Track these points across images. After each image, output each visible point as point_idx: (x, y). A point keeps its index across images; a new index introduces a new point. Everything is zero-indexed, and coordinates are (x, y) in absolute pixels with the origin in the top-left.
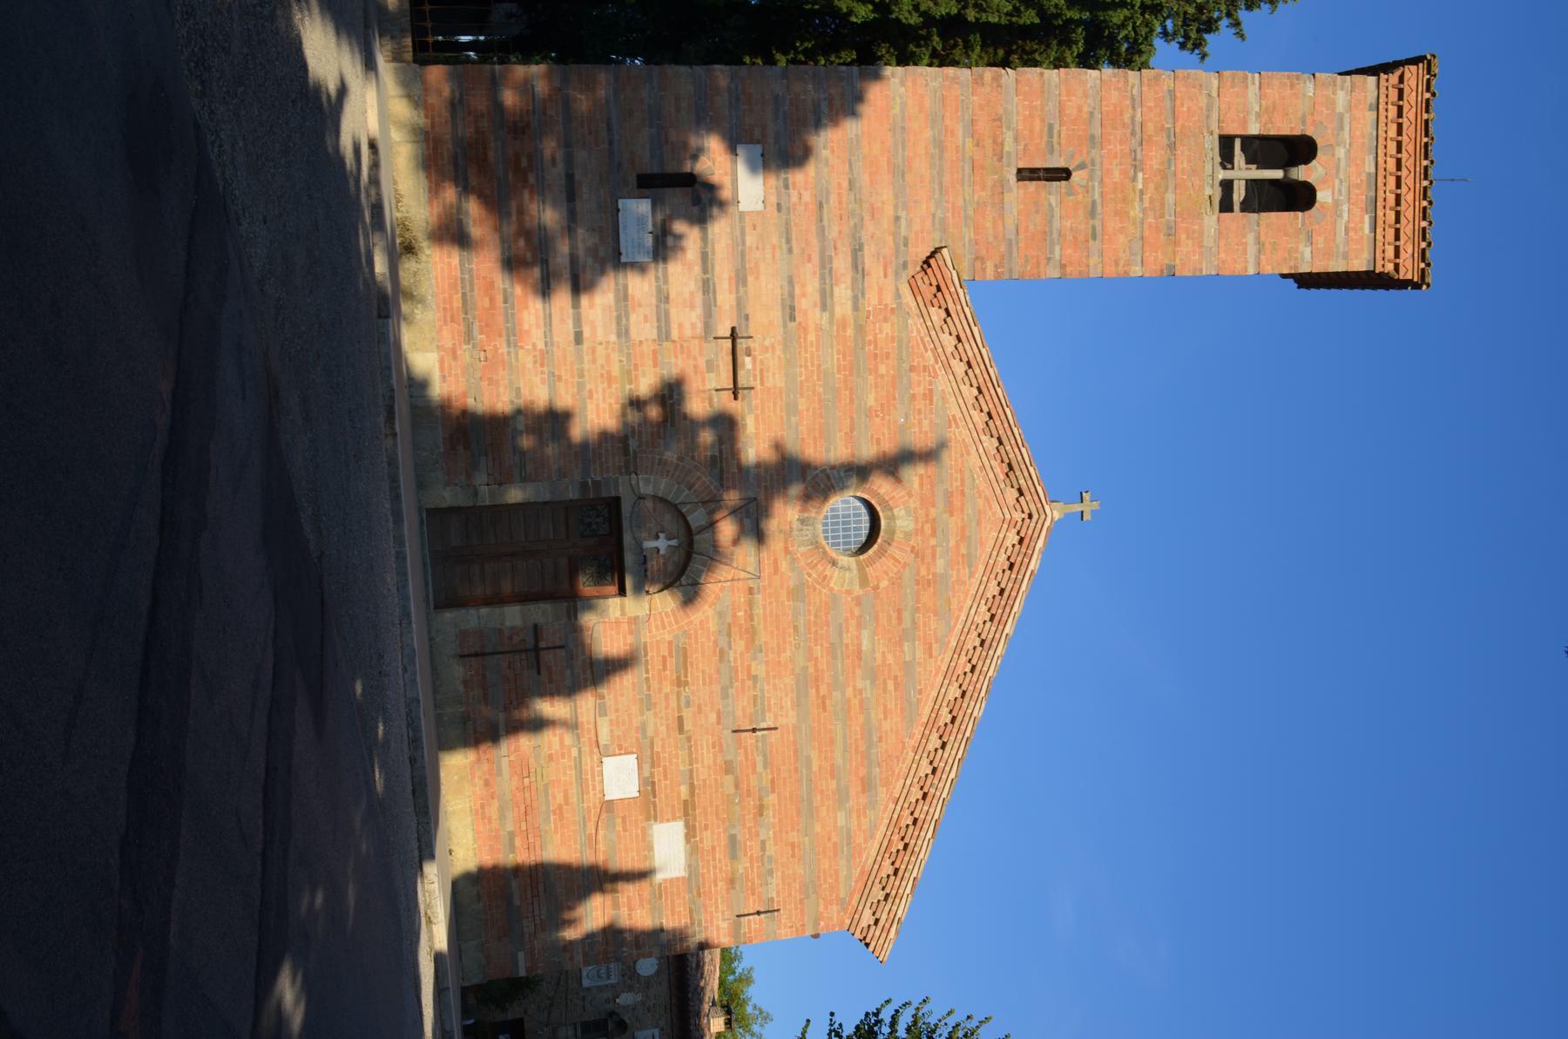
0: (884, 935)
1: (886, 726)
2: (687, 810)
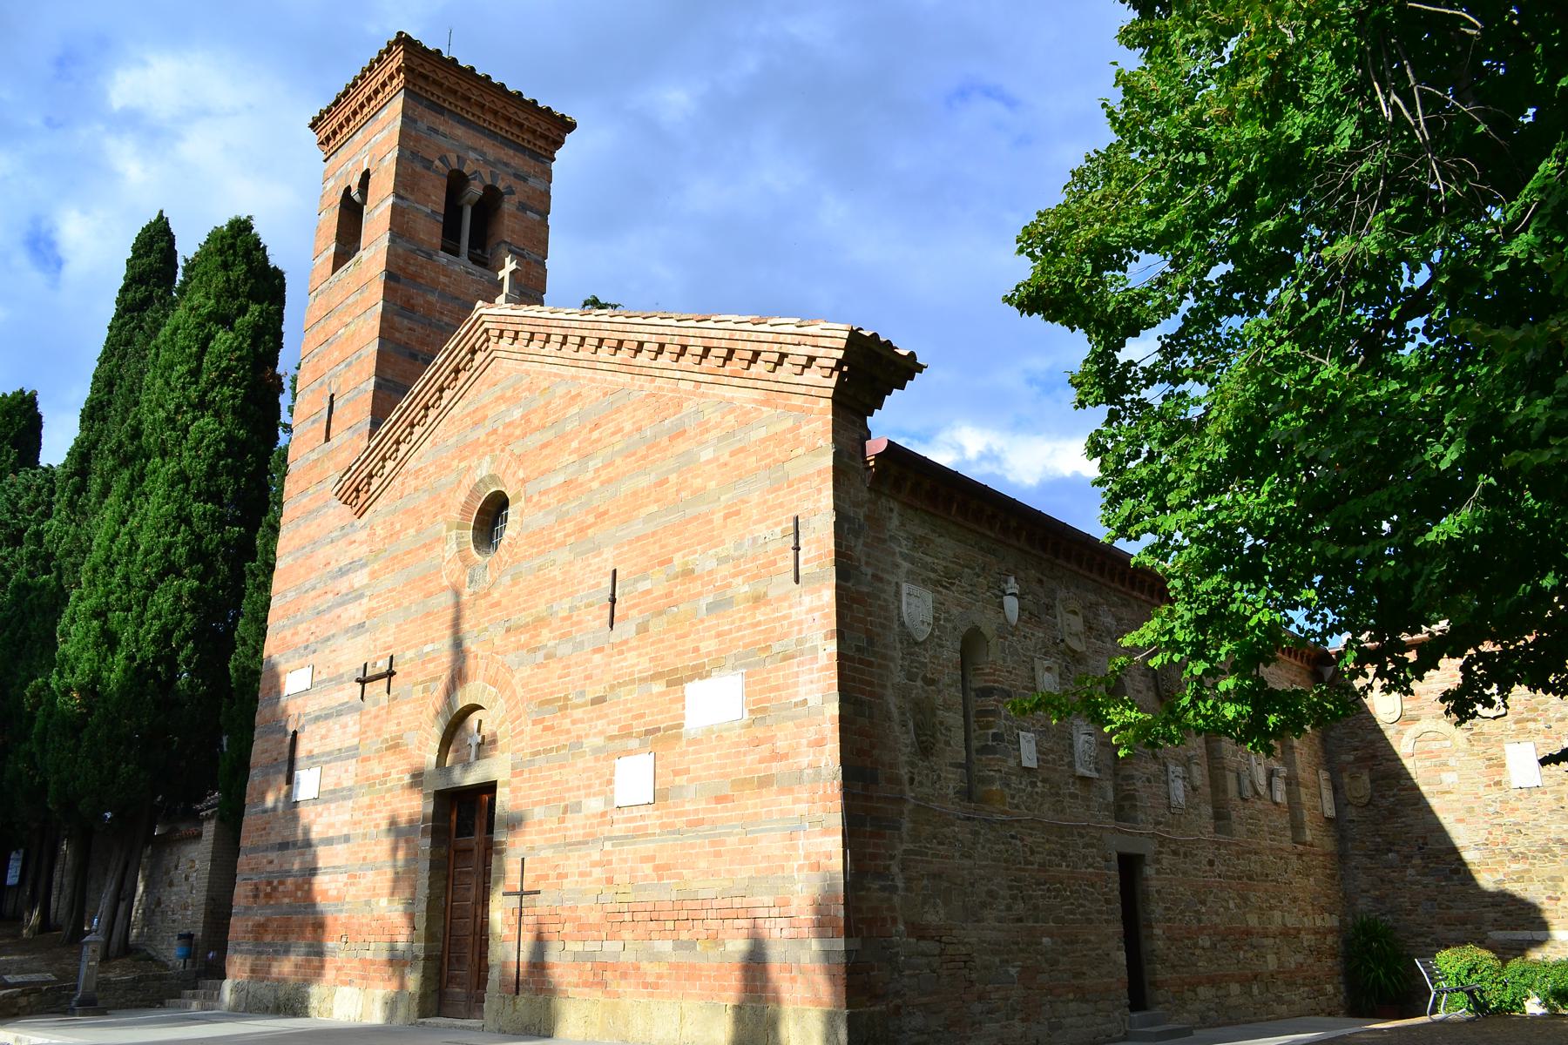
0: (821, 342)
1: (628, 427)
2: (676, 680)
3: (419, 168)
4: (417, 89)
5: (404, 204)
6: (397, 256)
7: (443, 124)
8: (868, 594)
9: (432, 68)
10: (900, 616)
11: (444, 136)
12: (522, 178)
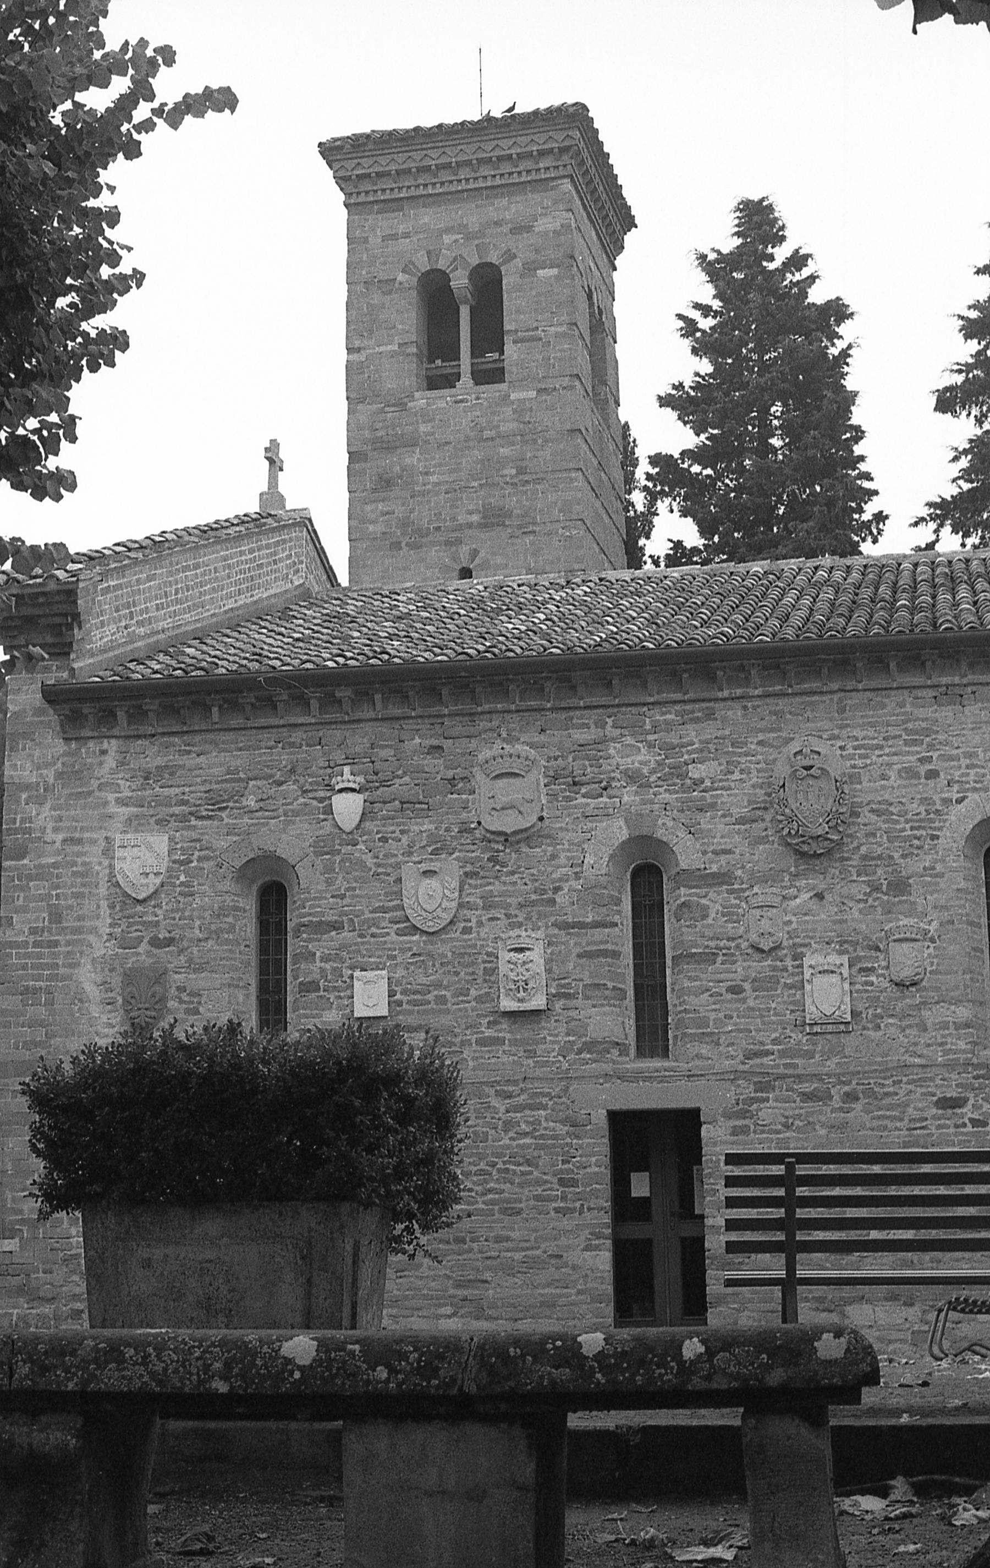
3: (376, 298)
4: (362, 198)
5: (361, 357)
6: (360, 428)
7: (399, 223)
8: (55, 865)
9: (371, 161)
10: (112, 875)
11: (407, 235)
12: (520, 229)
